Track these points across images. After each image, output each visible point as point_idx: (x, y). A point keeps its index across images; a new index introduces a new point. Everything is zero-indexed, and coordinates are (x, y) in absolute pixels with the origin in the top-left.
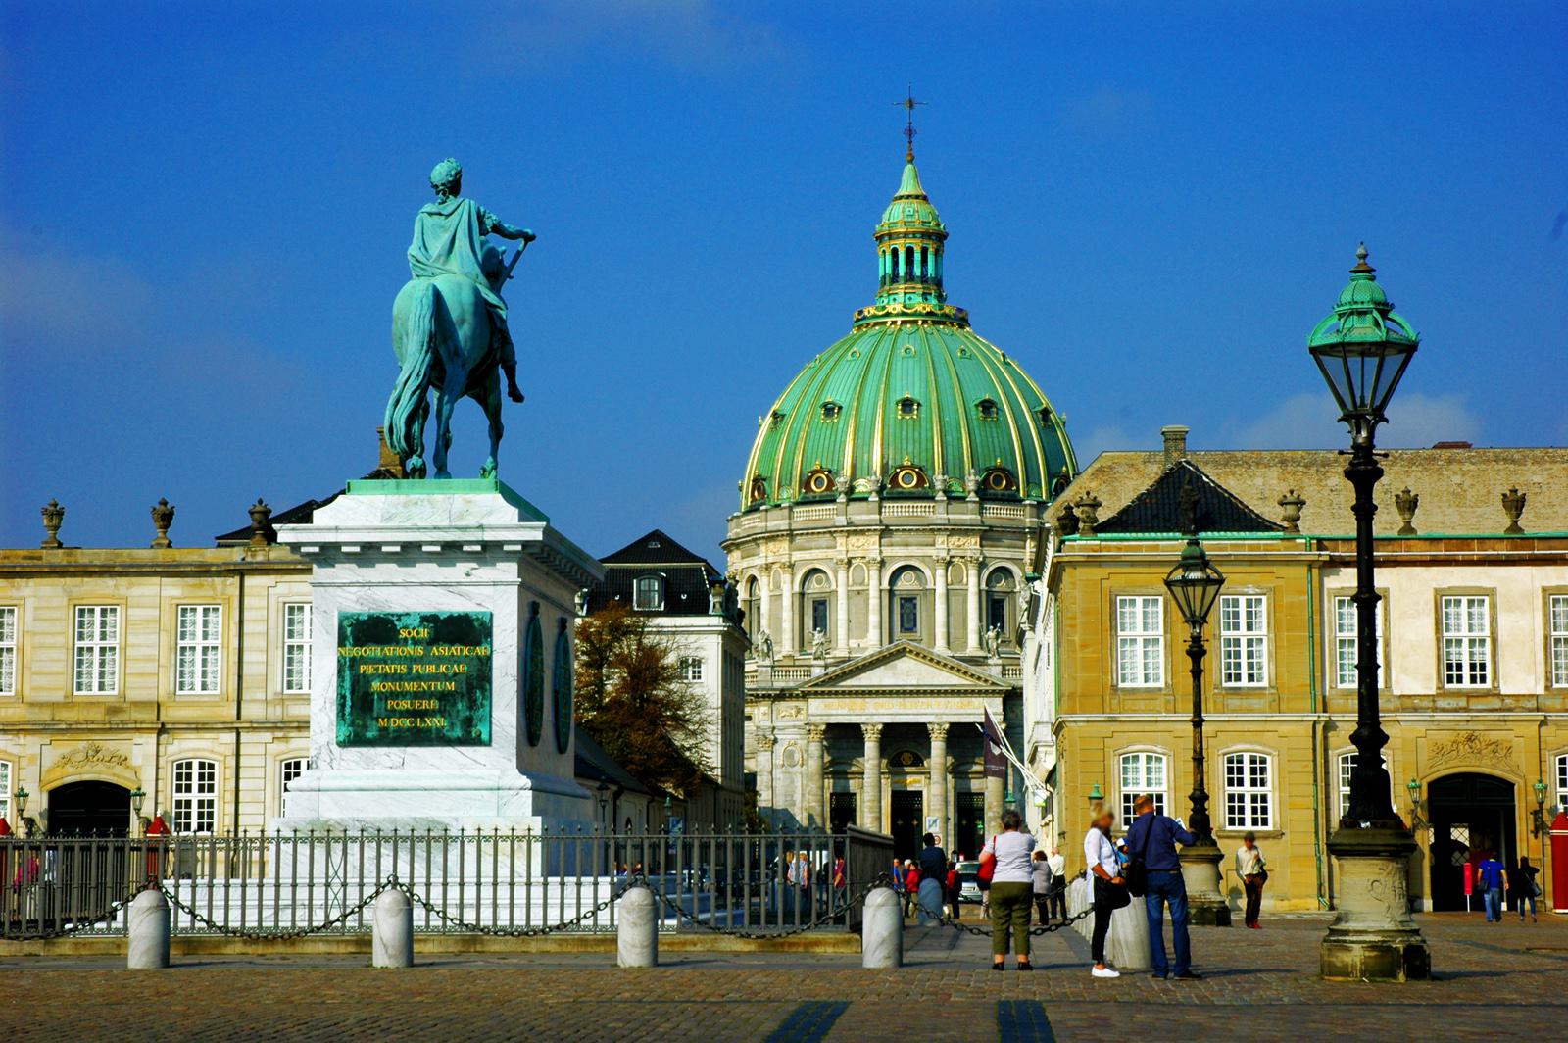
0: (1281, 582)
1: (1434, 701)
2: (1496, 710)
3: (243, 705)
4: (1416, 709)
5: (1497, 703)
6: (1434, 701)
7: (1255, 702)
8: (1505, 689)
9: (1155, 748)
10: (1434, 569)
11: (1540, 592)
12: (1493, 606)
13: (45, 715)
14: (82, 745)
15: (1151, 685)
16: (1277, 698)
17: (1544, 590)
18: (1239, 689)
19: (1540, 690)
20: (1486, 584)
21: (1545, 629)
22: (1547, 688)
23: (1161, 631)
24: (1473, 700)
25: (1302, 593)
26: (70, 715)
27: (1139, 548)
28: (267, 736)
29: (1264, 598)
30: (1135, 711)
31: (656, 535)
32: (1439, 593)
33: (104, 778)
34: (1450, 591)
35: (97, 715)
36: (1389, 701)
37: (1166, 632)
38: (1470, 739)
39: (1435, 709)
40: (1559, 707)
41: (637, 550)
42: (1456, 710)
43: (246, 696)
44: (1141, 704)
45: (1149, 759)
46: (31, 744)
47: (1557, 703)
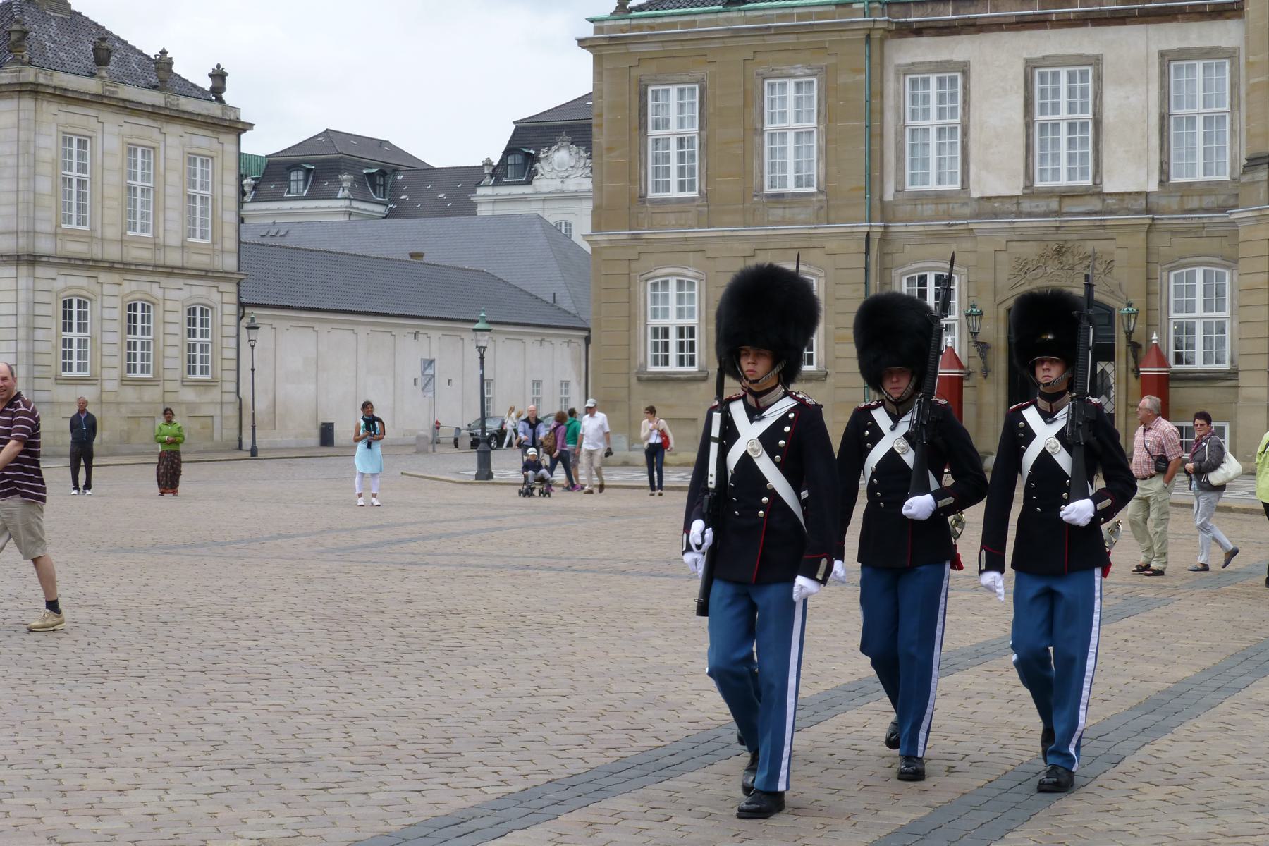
0: (833, 60)
1: (1018, 204)
2: (1095, 213)
4: (995, 215)
5: (1096, 204)
6: (1018, 204)
7: (801, 213)
8: (1108, 187)
9: (685, 271)
10: (1025, 35)
11: (1157, 55)
12: (1098, 79)
15: (687, 194)
16: (826, 203)
17: (1162, 55)
18: (782, 195)
19: (1153, 186)
20: (1090, 50)
21: (1161, 107)
22: (1161, 183)
23: (696, 129)
24: (1066, 201)
25: (857, 71)
27: (674, 25)
29: (814, 80)
30: (666, 227)
32: (1030, 66)
34: (1045, 61)
36: (965, 204)
37: (701, 128)
38: (1060, 252)
39: (1019, 214)
40: (1175, 207)
42: (1045, 215)
44: (672, 218)
45: (680, 283)
47: (1174, 203)
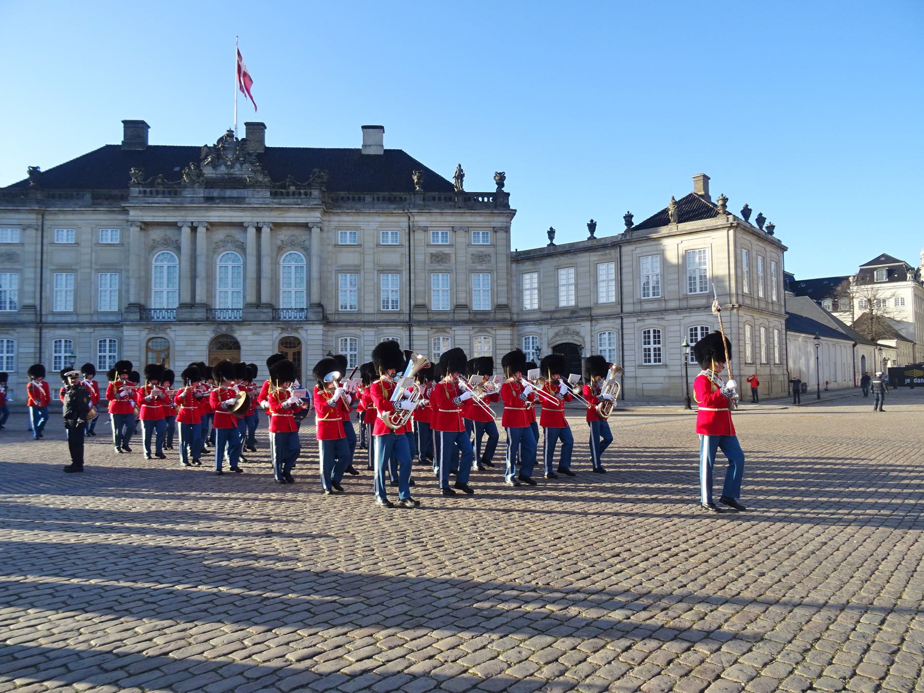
3: (624, 306)
13: (549, 316)
14: (562, 328)
26: (557, 315)
28: (635, 320)
31: (883, 255)
33: (571, 341)
35: (566, 314)
41: (876, 261)
43: (625, 301)
46: (545, 328)
